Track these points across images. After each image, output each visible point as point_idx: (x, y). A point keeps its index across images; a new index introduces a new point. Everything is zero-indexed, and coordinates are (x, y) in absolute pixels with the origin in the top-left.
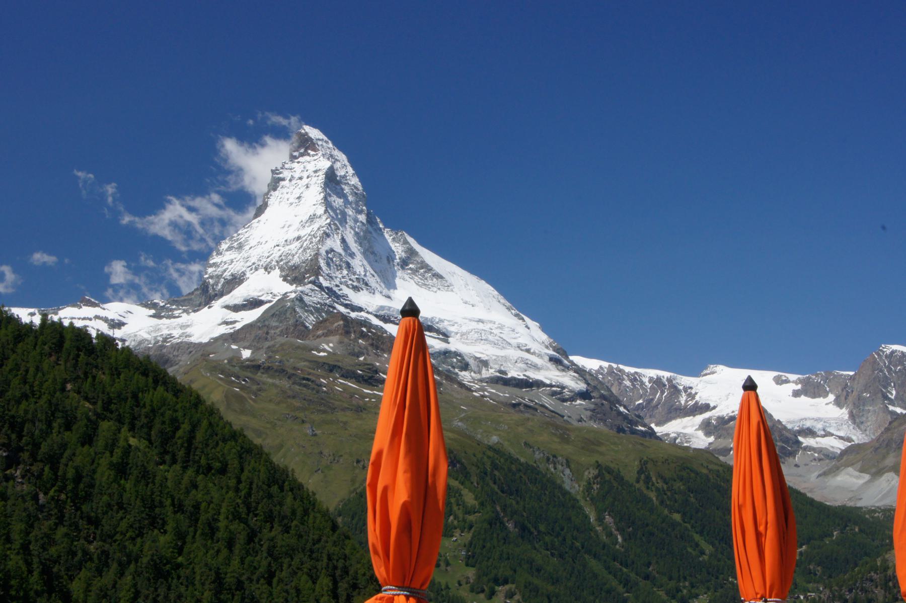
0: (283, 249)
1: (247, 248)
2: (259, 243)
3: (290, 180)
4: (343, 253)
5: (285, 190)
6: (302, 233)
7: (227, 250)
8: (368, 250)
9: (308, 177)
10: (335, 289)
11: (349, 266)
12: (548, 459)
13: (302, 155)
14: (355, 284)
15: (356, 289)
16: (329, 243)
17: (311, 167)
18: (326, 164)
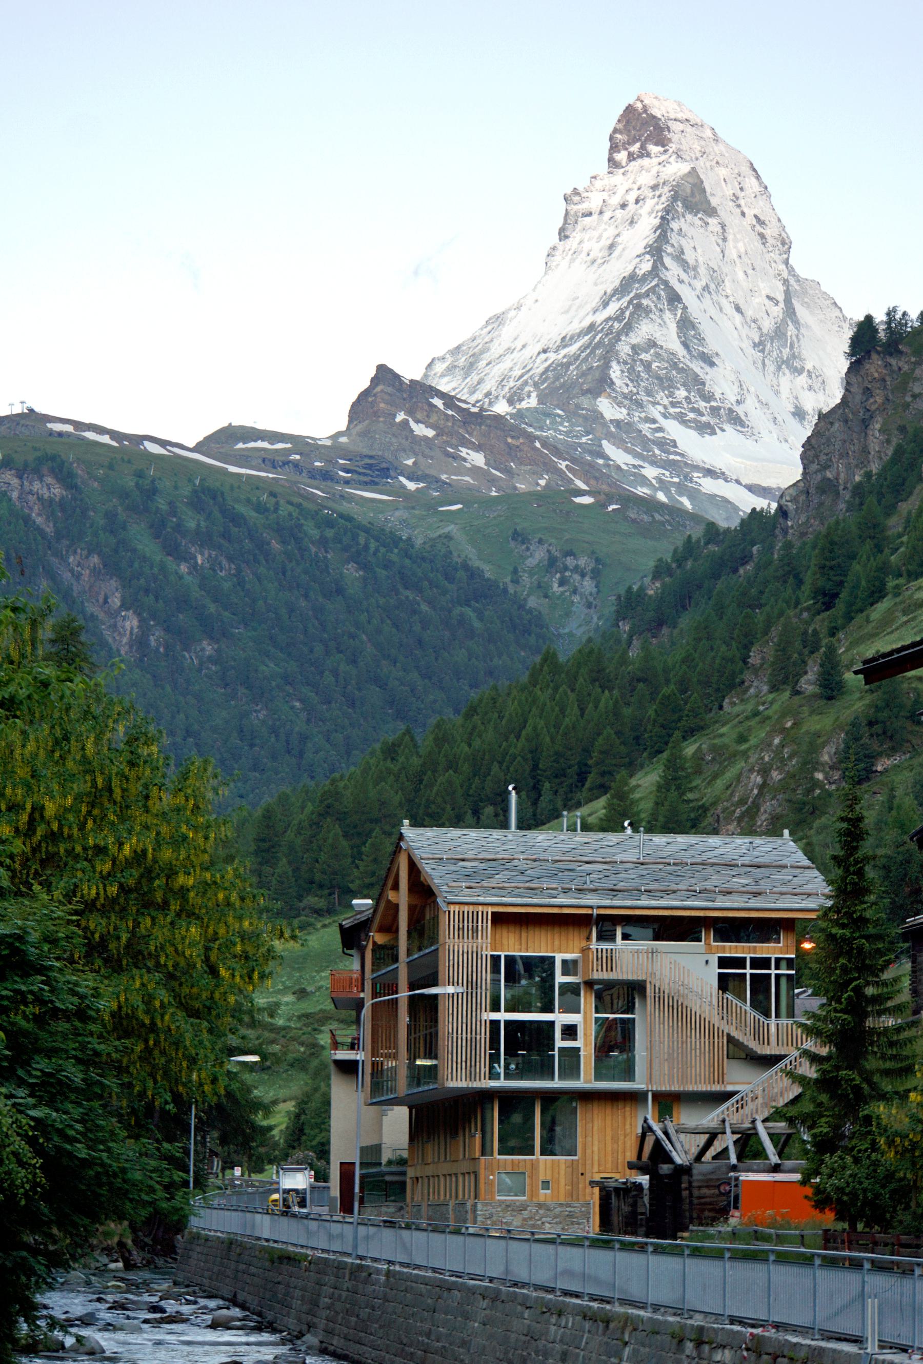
0: (552, 356)
1: (483, 363)
2: (510, 350)
3: (601, 213)
4: (681, 351)
5: (586, 236)
6: (600, 317)
7: (442, 376)
8: (786, 362)
9: (637, 202)
10: (645, 428)
11: (696, 383)
12: (552, 562)
13: (631, 157)
14: (703, 419)
15: (705, 429)
16: (645, 330)
17: (647, 179)
18: (676, 169)
